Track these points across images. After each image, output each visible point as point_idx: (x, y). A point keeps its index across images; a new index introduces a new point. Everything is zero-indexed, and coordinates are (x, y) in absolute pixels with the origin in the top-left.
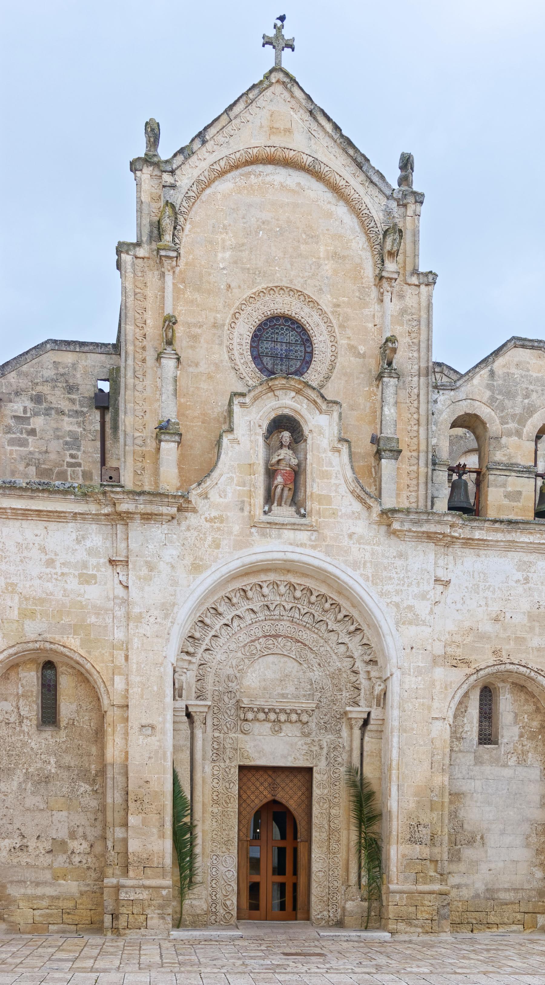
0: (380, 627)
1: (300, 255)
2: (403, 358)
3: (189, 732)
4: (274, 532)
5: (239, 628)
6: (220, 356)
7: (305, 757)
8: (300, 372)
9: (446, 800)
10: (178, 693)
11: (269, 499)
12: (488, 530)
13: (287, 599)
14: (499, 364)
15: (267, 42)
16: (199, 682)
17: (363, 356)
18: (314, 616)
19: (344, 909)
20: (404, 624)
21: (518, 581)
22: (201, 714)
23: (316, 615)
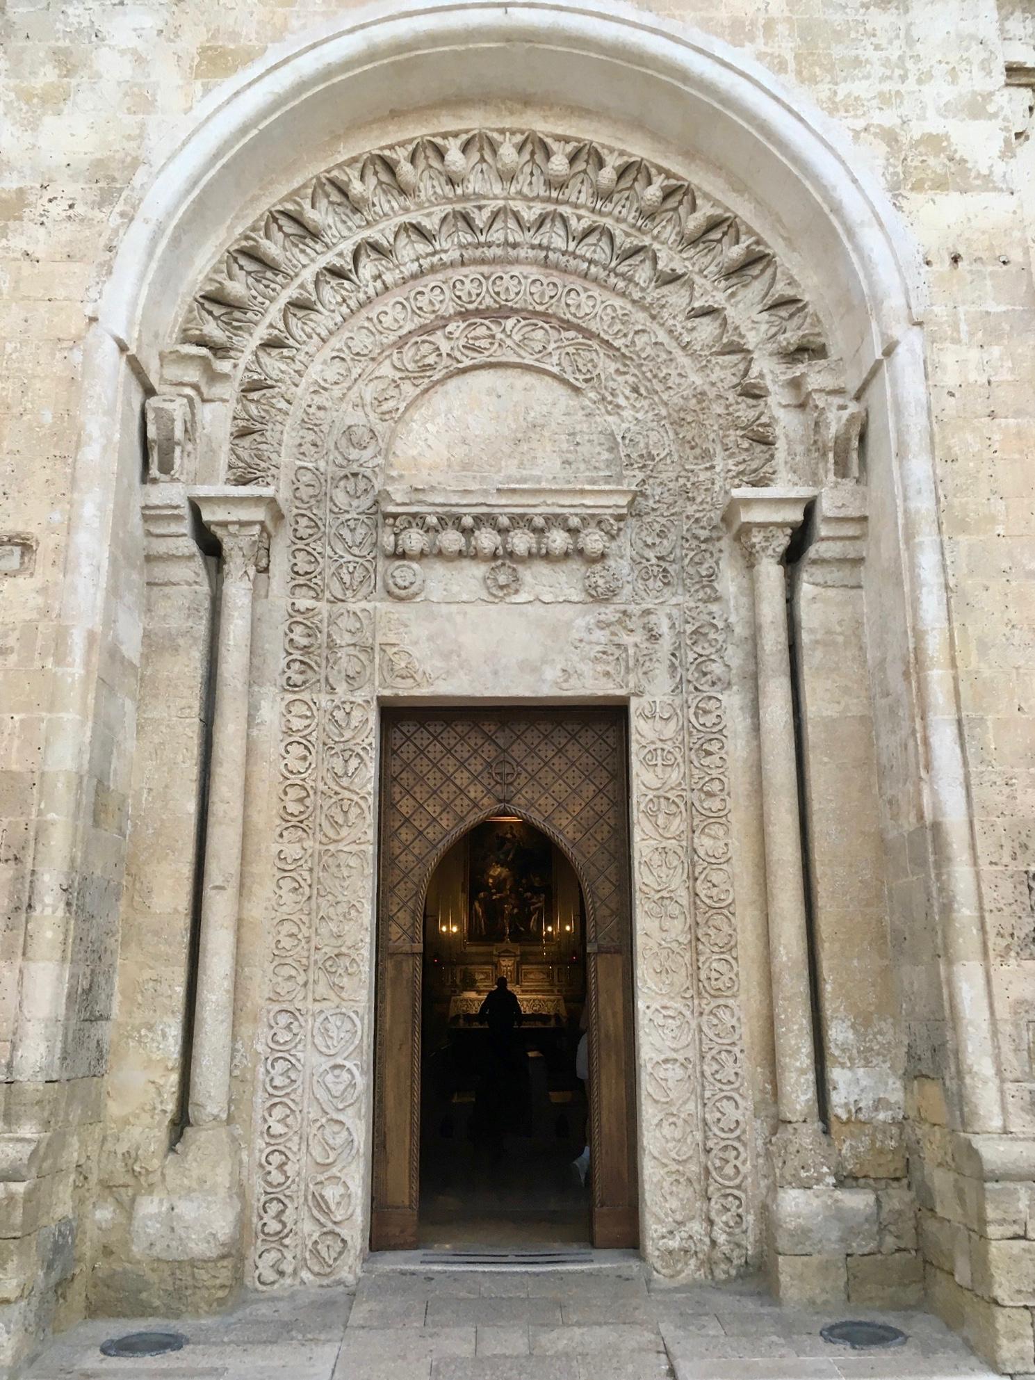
0: (837, 209)
3: (205, 589)
5: (379, 284)
7: (600, 668)
10: (153, 453)
13: (526, 190)
16: (246, 442)
18: (612, 238)
19: (766, 1214)
20: (918, 187)
22: (247, 531)
23: (617, 232)
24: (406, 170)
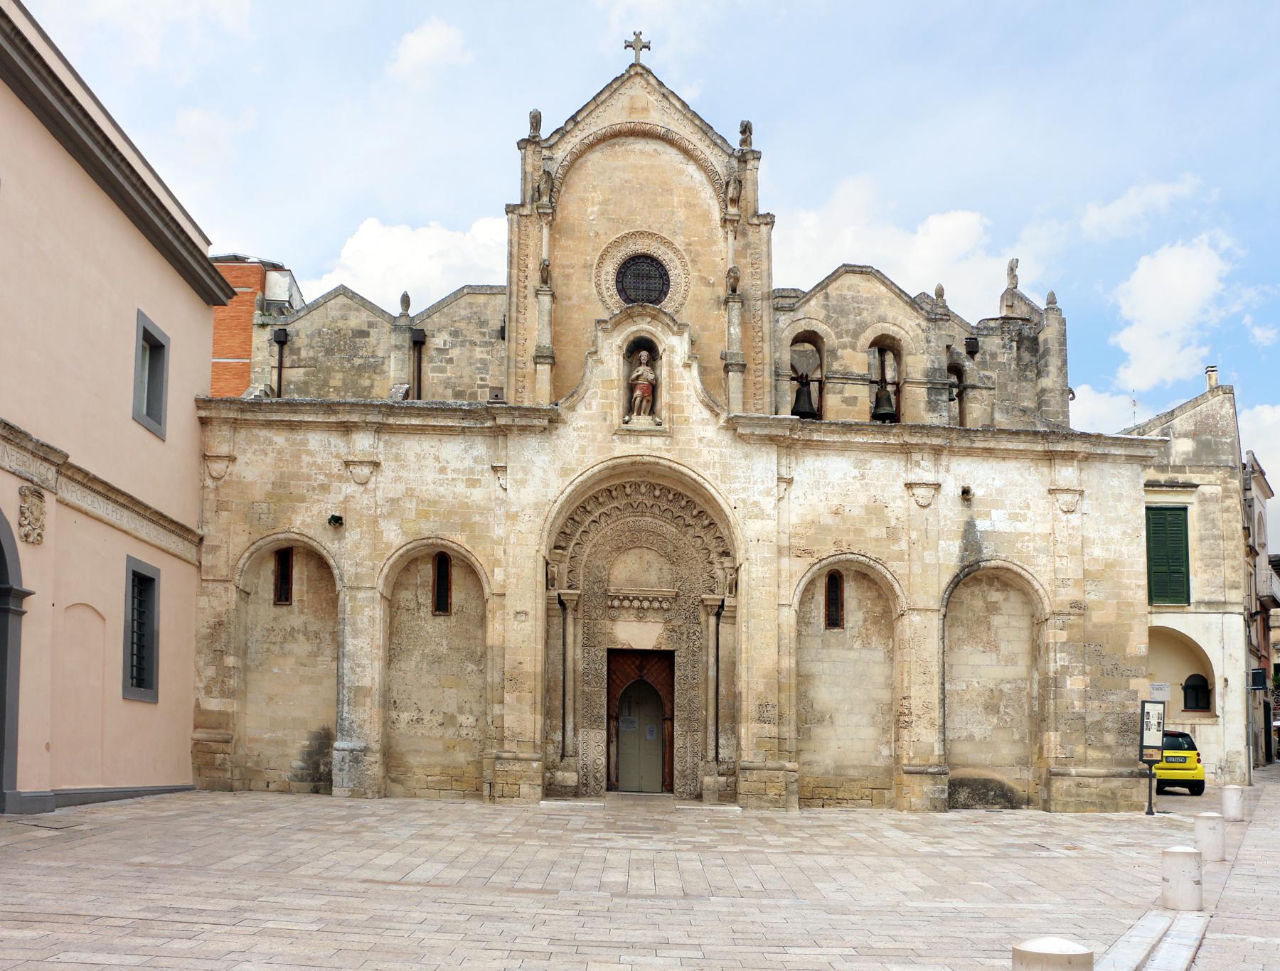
1: (657, 206)
2: (745, 284)
4: (633, 439)
6: (593, 291)
8: (658, 301)
9: (793, 681)
10: (550, 582)
11: (630, 409)
12: (825, 432)
14: (832, 289)
15: (628, 45)
17: (713, 285)
21: (855, 477)
24: (614, 493)
